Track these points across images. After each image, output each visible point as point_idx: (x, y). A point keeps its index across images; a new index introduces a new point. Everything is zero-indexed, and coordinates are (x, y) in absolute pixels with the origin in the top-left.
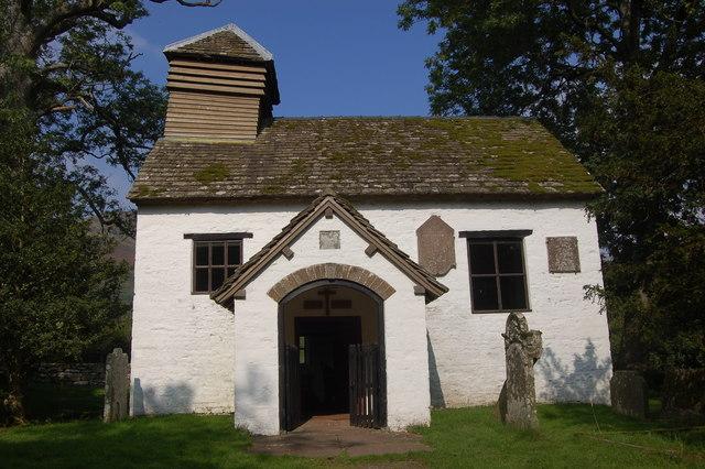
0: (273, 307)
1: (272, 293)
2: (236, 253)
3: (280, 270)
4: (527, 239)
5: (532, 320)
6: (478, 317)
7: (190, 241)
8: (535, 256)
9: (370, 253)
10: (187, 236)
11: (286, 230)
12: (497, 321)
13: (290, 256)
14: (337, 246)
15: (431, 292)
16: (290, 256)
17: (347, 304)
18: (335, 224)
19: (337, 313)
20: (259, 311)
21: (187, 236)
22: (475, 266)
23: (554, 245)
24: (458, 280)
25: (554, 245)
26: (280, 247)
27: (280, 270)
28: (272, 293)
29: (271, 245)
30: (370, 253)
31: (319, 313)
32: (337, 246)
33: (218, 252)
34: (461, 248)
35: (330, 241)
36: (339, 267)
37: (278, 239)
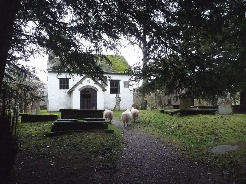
0: (79, 92)
1: (79, 90)
2: (68, 82)
3: (80, 86)
4: (120, 81)
5: (120, 95)
6: (111, 95)
7: (59, 79)
8: (121, 84)
9: (95, 84)
10: (58, 78)
11: (81, 80)
12: (114, 95)
13: (81, 83)
14: (90, 82)
15: (104, 90)
16: (81, 83)
17: (88, 92)
18: (88, 79)
19: (86, 93)
20: (77, 94)
21: (58, 78)
22: (111, 85)
23: (125, 82)
24: (108, 88)
25: (125, 82)
26: (80, 82)
27: (80, 86)
28: (79, 90)
29: (79, 82)
30: (95, 84)
31: (84, 93)
32: (90, 82)
33: (64, 82)
34: (108, 83)
35: (89, 81)
36: (90, 86)
37: (80, 81)
